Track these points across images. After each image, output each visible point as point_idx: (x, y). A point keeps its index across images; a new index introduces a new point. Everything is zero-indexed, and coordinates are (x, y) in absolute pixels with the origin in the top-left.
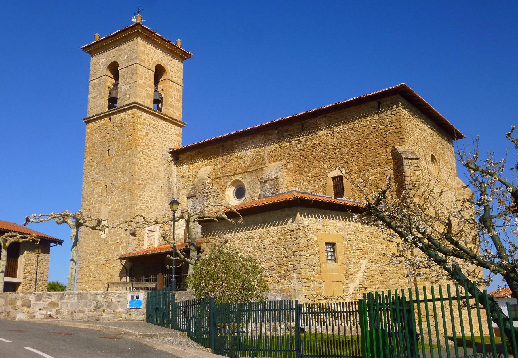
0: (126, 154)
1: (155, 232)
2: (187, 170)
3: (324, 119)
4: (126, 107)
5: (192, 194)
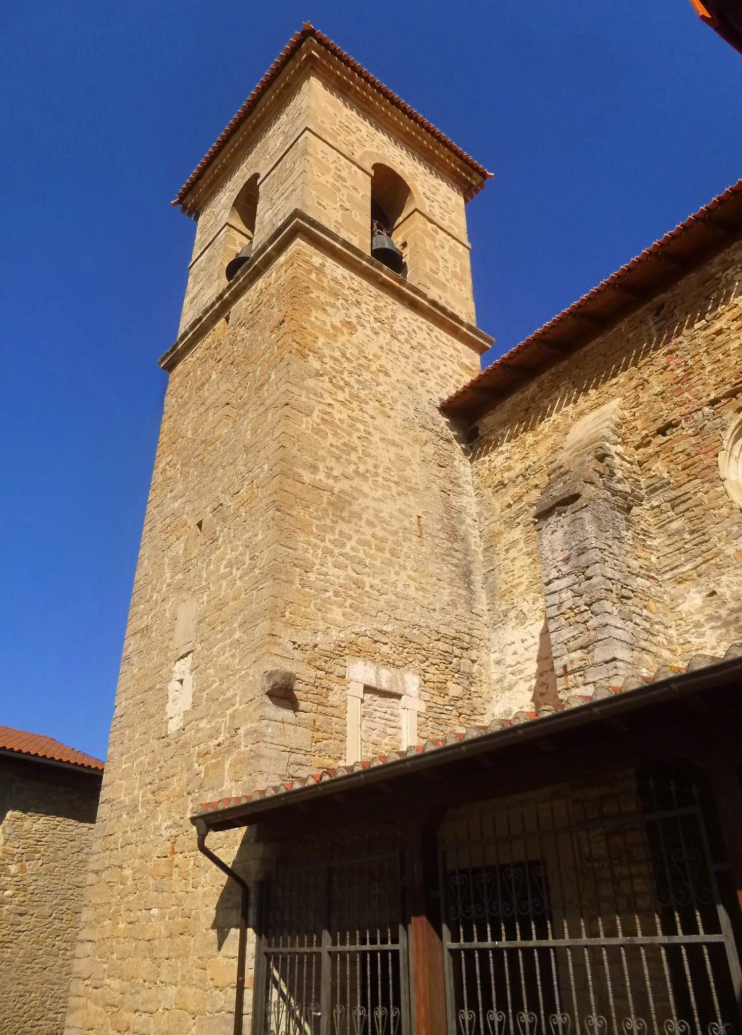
1: (399, 696)
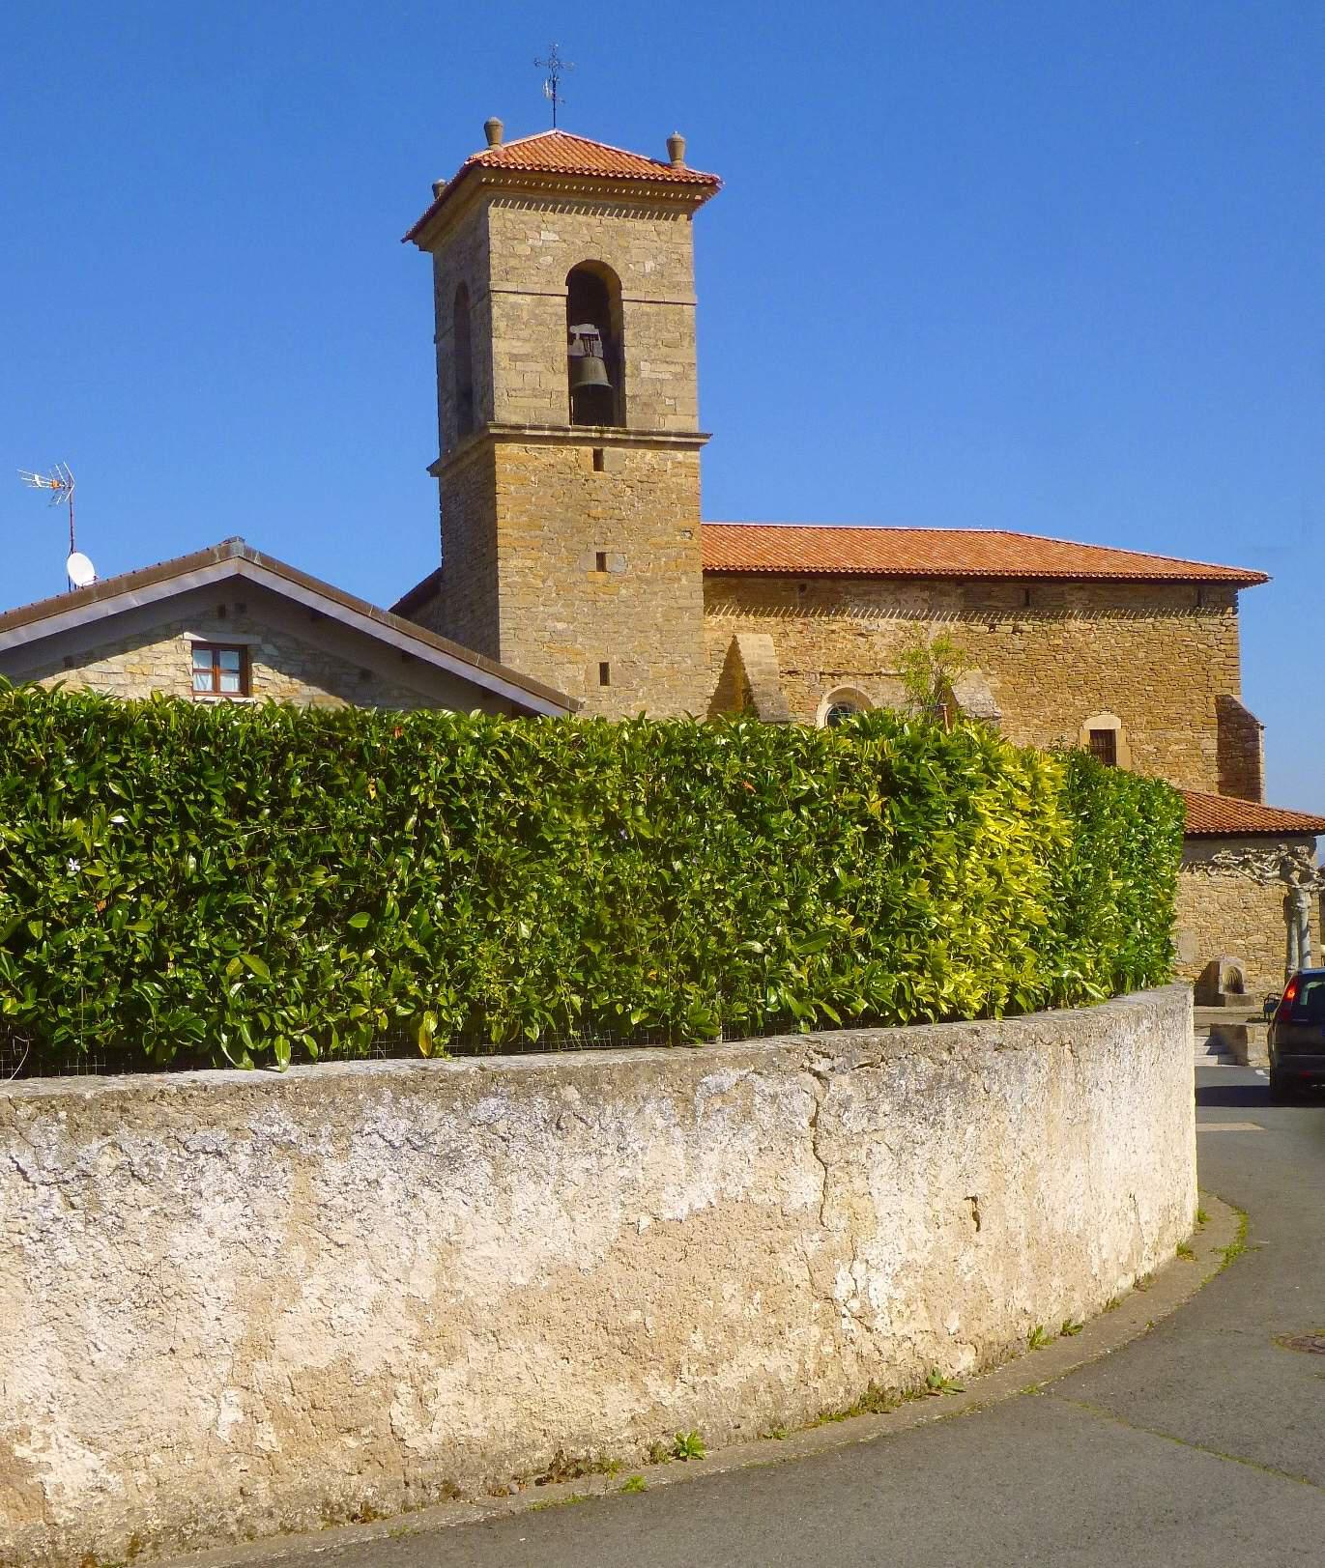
3: (1081, 594)
4: (673, 439)
5: (773, 715)
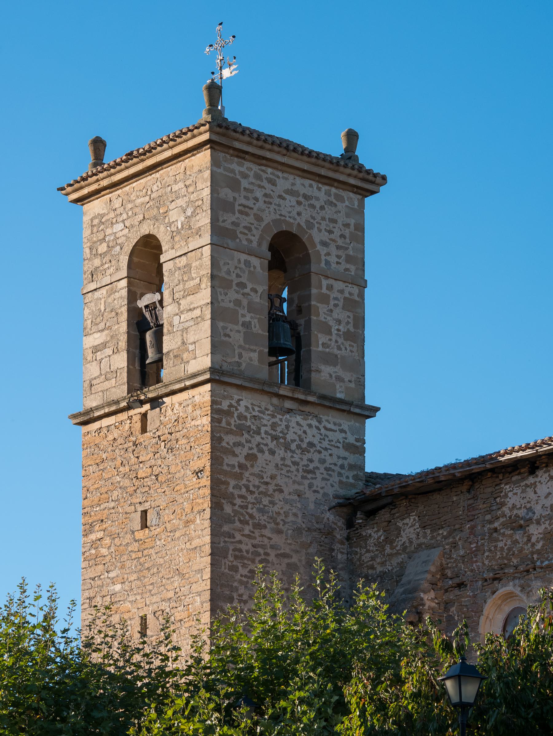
0: (192, 526)
2: (379, 560)
